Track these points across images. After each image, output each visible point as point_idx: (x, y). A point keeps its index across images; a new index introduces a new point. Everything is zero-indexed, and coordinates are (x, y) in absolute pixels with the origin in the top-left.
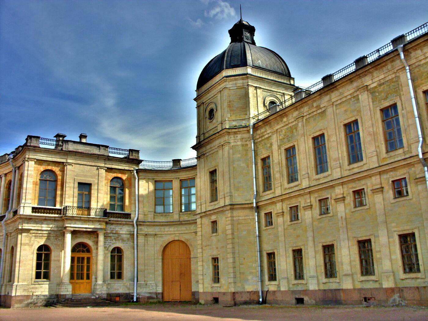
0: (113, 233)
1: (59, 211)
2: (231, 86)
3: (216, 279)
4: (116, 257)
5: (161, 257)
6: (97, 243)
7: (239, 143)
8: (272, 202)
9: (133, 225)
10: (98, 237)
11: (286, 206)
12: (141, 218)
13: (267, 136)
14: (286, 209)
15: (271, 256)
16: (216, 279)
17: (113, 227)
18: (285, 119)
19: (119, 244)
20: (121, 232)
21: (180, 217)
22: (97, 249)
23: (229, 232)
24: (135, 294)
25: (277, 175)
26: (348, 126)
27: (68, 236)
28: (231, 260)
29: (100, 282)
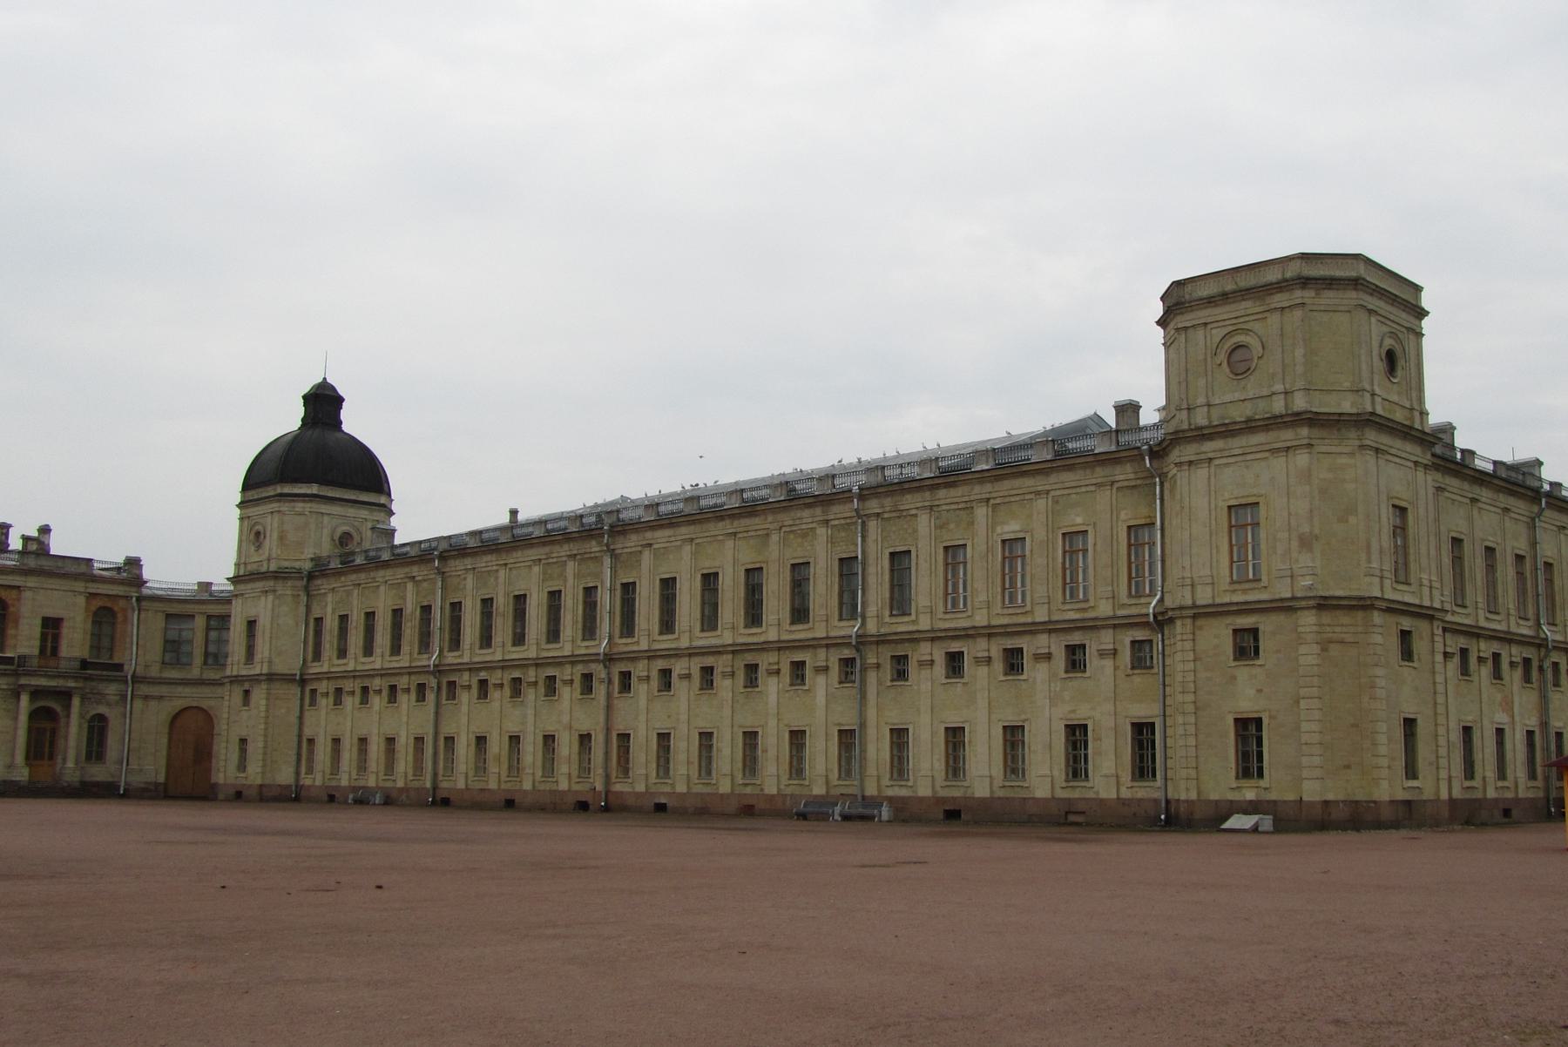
0: (94, 694)
1: (10, 660)
2: (286, 509)
3: (242, 766)
4: (96, 728)
5: (167, 731)
6: (68, 707)
7: (289, 592)
8: (319, 677)
9: (126, 682)
10: (70, 699)
11: (332, 686)
12: (140, 671)
13: (323, 591)
14: (332, 690)
15: (311, 741)
16: (242, 766)
17: (94, 684)
18: (343, 579)
19: (102, 709)
20: (107, 692)
21: (201, 674)
22: (68, 716)
23: (263, 708)
24: (122, 784)
25: (327, 646)
26: (395, 611)
27: (25, 699)
28: (261, 745)
29: (70, 764)
